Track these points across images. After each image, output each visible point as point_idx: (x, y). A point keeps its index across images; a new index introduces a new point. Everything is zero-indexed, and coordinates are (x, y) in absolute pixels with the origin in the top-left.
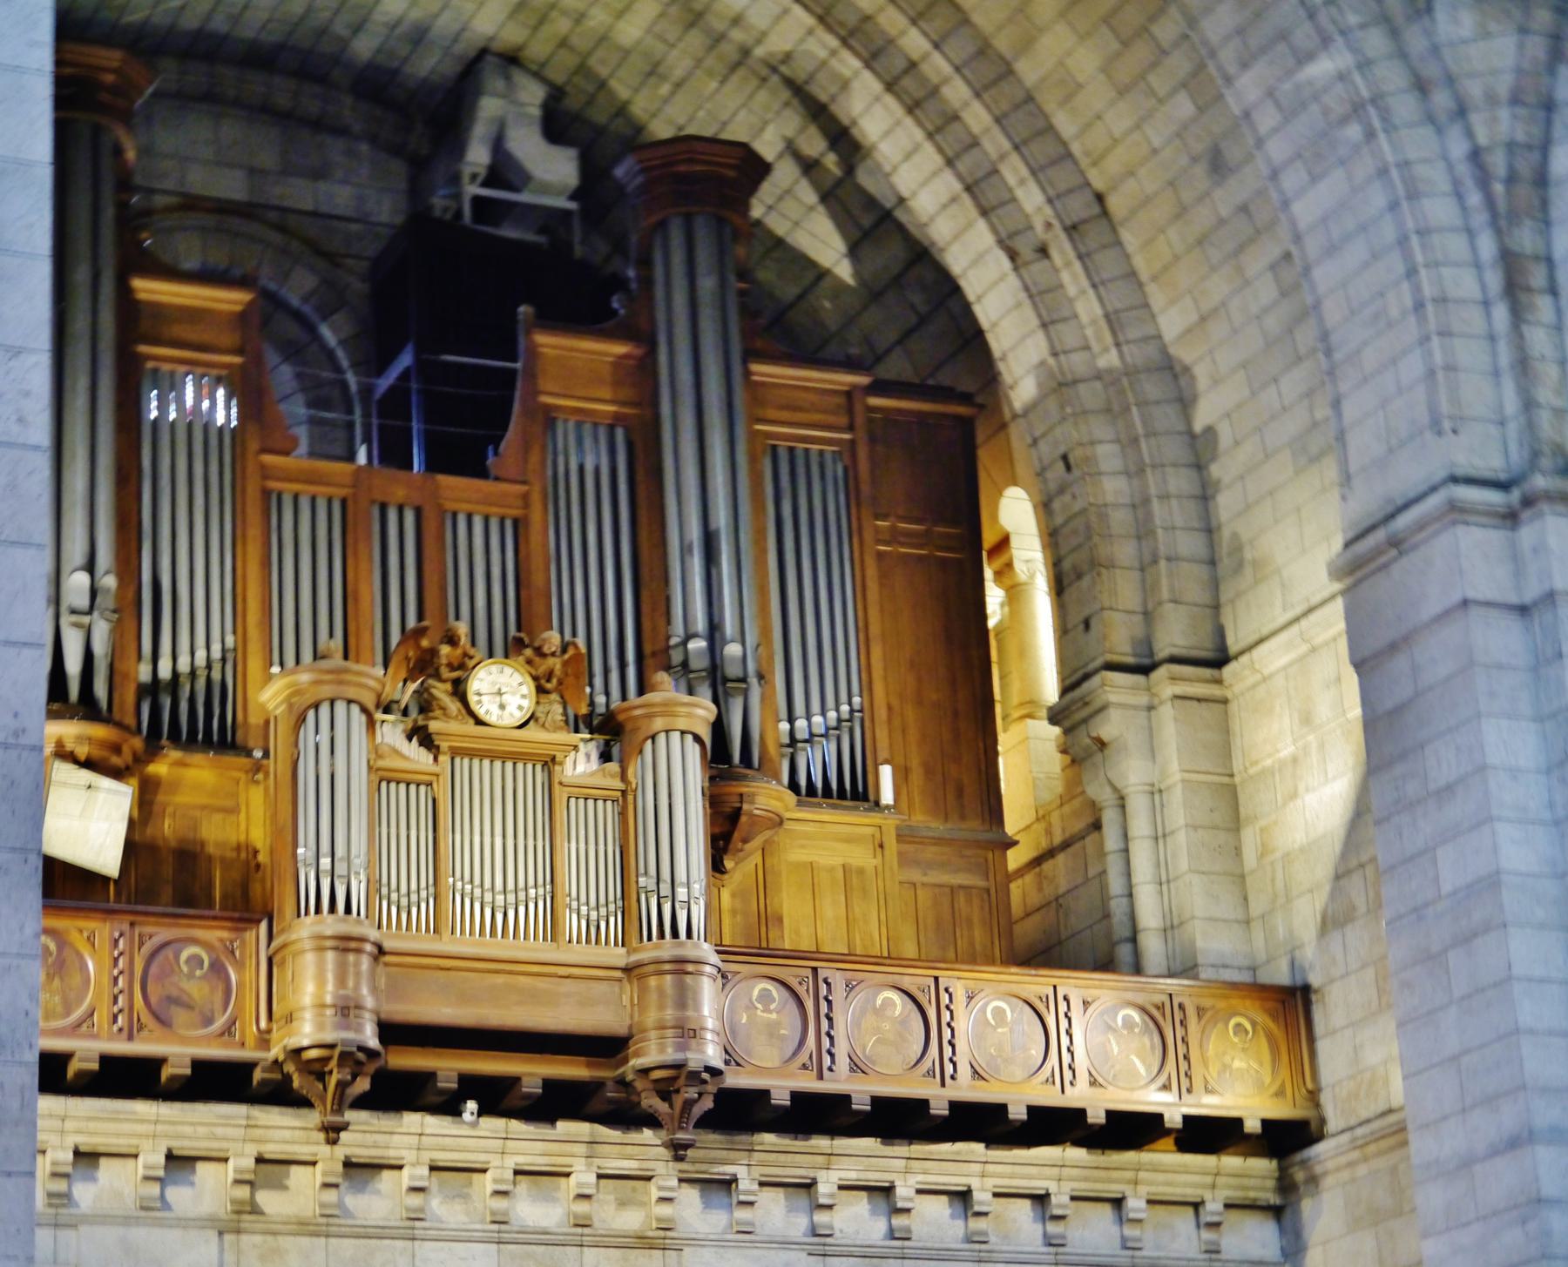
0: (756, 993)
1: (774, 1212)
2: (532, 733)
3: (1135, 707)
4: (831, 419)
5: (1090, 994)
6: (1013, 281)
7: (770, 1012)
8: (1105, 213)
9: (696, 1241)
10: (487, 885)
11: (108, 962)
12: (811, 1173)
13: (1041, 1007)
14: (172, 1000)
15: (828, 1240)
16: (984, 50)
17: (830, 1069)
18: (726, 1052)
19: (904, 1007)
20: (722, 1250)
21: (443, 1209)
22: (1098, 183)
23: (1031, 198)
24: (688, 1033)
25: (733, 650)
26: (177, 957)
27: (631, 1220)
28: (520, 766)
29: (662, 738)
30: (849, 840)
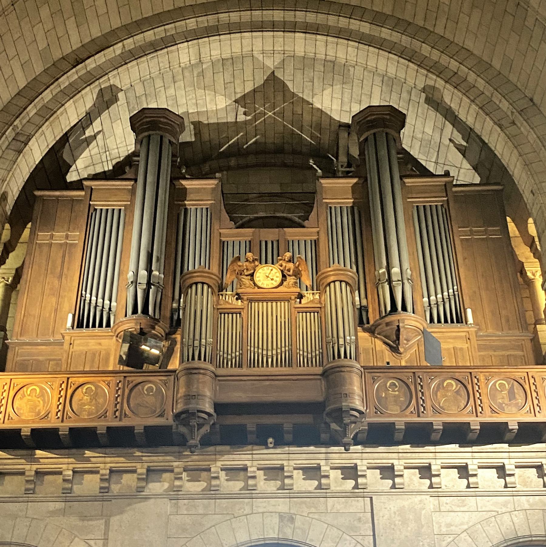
0: (388, 384)
2: (281, 289)
6: (502, 134)
7: (395, 391)
8: (534, 104)
10: (265, 347)
11: (114, 392)
13: (522, 382)
15: (439, 490)
16: (480, 60)
17: (423, 412)
18: (376, 409)
19: (457, 386)
20: (390, 497)
22: (529, 95)
23: (505, 105)
25: (395, 270)
26: (143, 389)
28: (279, 303)
29: (332, 285)
30: (455, 338)
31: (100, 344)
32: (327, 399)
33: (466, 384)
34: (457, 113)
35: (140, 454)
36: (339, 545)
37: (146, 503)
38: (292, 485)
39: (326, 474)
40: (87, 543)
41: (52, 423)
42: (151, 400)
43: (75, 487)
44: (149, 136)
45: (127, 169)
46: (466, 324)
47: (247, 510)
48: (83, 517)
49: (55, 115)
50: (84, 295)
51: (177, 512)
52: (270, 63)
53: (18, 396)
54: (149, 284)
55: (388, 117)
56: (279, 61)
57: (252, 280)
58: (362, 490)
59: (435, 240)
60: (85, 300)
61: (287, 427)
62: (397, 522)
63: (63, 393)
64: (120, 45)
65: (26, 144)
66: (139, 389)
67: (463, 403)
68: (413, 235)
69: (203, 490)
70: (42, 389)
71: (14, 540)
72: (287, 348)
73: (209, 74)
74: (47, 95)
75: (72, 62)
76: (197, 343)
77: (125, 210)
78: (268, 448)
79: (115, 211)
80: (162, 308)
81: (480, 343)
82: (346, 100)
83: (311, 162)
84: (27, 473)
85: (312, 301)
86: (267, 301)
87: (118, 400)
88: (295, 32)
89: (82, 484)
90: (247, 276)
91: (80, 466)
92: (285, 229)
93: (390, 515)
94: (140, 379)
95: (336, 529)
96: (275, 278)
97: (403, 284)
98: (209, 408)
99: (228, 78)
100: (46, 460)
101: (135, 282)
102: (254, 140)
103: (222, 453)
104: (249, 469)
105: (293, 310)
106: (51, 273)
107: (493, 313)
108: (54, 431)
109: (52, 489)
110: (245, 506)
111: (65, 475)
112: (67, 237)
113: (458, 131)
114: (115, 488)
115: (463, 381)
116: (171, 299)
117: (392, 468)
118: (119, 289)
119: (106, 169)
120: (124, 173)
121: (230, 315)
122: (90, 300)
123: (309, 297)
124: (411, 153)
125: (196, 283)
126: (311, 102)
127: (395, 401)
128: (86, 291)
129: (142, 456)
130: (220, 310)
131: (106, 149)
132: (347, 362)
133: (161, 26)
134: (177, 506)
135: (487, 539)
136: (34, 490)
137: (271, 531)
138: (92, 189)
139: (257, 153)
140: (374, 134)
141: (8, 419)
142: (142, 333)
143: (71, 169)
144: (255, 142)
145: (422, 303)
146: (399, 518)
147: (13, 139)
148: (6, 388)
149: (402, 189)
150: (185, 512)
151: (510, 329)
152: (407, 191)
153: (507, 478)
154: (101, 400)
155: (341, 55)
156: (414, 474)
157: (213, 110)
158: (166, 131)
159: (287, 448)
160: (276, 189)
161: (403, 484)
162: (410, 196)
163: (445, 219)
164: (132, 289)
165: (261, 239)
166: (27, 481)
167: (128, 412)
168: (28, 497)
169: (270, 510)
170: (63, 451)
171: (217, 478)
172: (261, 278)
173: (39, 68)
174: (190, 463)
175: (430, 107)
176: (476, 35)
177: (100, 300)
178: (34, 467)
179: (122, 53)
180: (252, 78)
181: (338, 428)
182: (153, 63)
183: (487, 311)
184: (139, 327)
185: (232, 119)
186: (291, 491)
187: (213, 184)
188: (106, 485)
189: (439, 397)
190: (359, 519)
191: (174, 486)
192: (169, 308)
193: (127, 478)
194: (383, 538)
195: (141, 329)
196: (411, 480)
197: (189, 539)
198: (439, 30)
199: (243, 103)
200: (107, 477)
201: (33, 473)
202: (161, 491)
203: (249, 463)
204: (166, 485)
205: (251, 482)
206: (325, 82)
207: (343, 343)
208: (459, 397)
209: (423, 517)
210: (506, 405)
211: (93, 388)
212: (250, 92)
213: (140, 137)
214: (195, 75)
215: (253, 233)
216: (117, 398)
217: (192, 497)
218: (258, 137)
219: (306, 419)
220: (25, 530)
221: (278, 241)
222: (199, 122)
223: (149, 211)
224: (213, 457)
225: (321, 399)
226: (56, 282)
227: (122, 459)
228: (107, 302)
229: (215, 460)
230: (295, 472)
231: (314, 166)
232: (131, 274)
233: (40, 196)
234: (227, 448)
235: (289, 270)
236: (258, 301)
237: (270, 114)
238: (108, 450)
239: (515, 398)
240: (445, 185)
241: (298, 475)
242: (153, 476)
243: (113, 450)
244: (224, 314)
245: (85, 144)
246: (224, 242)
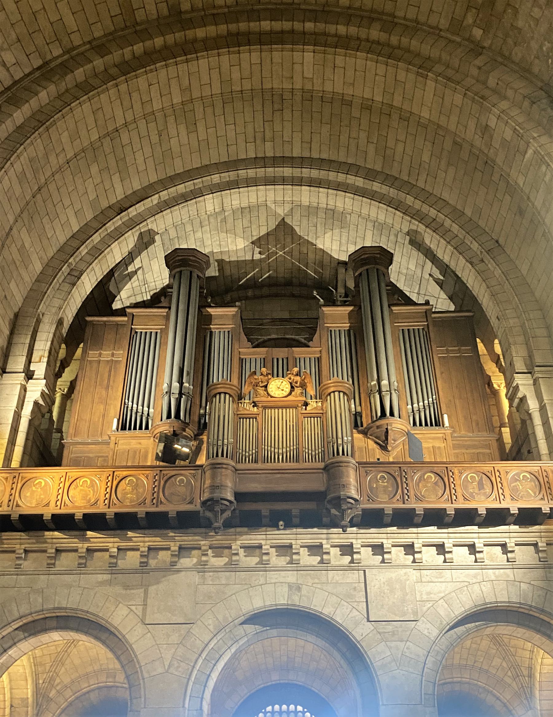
0: (379, 477)
3: (528, 385)
4: (421, 320)
5: (508, 469)
6: (473, 270)
7: (385, 483)
8: (499, 245)
10: (277, 446)
11: (152, 483)
13: (489, 475)
15: (421, 564)
16: (455, 209)
17: (407, 500)
19: (435, 478)
20: (380, 570)
22: (495, 238)
23: (475, 246)
25: (385, 382)
26: (176, 481)
29: (332, 394)
30: (434, 438)
31: (140, 443)
32: (328, 489)
33: (443, 476)
34: (435, 253)
35: (173, 534)
36: (338, 610)
37: (178, 575)
38: (299, 560)
39: (327, 551)
40: (129, 608)
41: (101, 509)
42: (182, 490)
43: (119, 562)
44: (181, 272)
45: (163, 299)
46: (443, 427)
47: (262, 581)
48: (126, 587)
49: (103, 255)
50: (126, 403)
51: (204, 582)
52: (280, 211)
53: (73, 486)
54: (181, 394)
55: (378, 256)
56: (288, 209)
57: (266, 390)
58: (357, 565)
59: (417, 357)
60: (128, 407)
61: (295, 512)
62: (386, 591)
63: (109, 484)
64: (157, 196)
65: (79, 278)
66: (172, 481)
67: (440, 493)
68: (399, 353)
69: (225, 565)
70: (92, 481)
72: (295, 447)
73: (230, 220)
74: (96, 238)
75: (117, 210)
76: (220, 443)
77: (161, 332)
78: (279, 529)
79: (153, 334)
80: (192, 414)
81: (454, 442)
82: (343, 241)
83: (315, 293)
84: (80, 551)
85: (315, 408)
86: (278, 408)
87: (155, 490)
88: (301, 185)
89: (125, 559)
90: (261, 387)
91: (123, 544)
92: (293, 349)
93: (380, 585)
94: (173, 473)
95: (335, 597)
96: (285, 389)
97: (391, 394)
98: (230, 496)
99: (246, 224)
100: (95, 540)
101: (169, 393)
102: (267, 275)
103: (241, 534)
104: (263, 547)
105: (300, 415)
106: (100, 385)
107: (465, 418)
108: (102, 516)
109: (101, 564)
110: (260, 577)
111: (111, 552)
112: (113, 355)
113: (436, 267)
114: (153, 563)
115: (441, 474)
116: (199, 406)
117: (382, 546)
118: (156, 398)
119: (145, 299)
120: (160, 302)
121: (248, 420)
122: (132, 407)
123: (313, 405)
124: (398, 285)
125: (220, 393)
126: (315, 243)
127: (385, 491)
128: (128, 400)
129: (175, 536)
130: (239, 416)
131: (145, 283)
132: (344, 459)
133: (191, 180)
134: (204, 578)
135: (460, 605)
136: (85, 564)
137: (281, 598)
138: (133, 315)
139: (270, 286)
140: (367, 270)
141: (64, 506)
142: (175, 434)
143: (116, 299)
144: (269, 277)
145: (407, 409)
146: (387, 588)
147: (68, 274)
148: (62, 479)
149: (390, 315)
150: (211, 583)
151: (479, 431)
152: (394, 317)
153: (477, 554)
155: (340, 205)
156: (400, 551)
157: (233, 250)
158: (195, 267)
159: (295, 530)
160: (286, 315)
161: (390, 559)
162: (396, 321)
163: (426, 340)
164: (166, 398)
165: (274, 357)
166: (80, 557)
167: (163, 499)
169: (281, 581)
170: (109, 532)
171: (237, 554)
172: (274, 389)
173: (89, 216)
174: (214, 542)
175: (413, 248)
176: (451, 188)
177: (140, 407)
178: (86, 545)
179: (158, 203)
180: (266, 224)
181: (337, 513)
182: (184, 211)
183: (460, 416)
184: (172, 430)
185: (248, 257)
186: (298, 565)
187: (233, 311)
188: (145, 560)
189: (420, 487)
190: (355, 589)
191: (201, 561)
192: (197, 414)
193: (162, 554)
194: (374, 604)
195: (174, 431)
196: (397, 555)
197: (212, 605)
198: (421, 184)
199: (258, 245)
200: (146, 553)
201: (85, 550)
202: (190, 565)
203: (263, 542)
204: (195, 560)
205: (265, 558)
206: (327, 227)
207: (341, 443)
208: (437, 487)
209: (407, 587)
210: (476, 494)
211: (135, 480)
212: (264, 235)
213: (173, 272)
214: (219, 221)
215: (267, 351)
216: (154, 488)
217: (216, 570)
218: (271, 272)
219: (311, 506)
220: (78, 597)
221: (287, 358)
222: (222, 260)
223: (181, 333)
224: (234, 537)
225: (323, 489)
226: (104, 392)
227: (158, 539)
228: (146, 409)
229: (236, 540)
230: (302, 549)
231: (318, 296)
232: (165, 385)
233: (91, 321)
234: (246, 529)
235: (296, 383)
236: (271, 408)
237: (281, 253)
238: (146, 531)
239: (483, 488)
240: (426, 312)
241: (304, 552)
242: (183, 553)
243: (151, 531)
245: (128, 278)
246: (242, 359)
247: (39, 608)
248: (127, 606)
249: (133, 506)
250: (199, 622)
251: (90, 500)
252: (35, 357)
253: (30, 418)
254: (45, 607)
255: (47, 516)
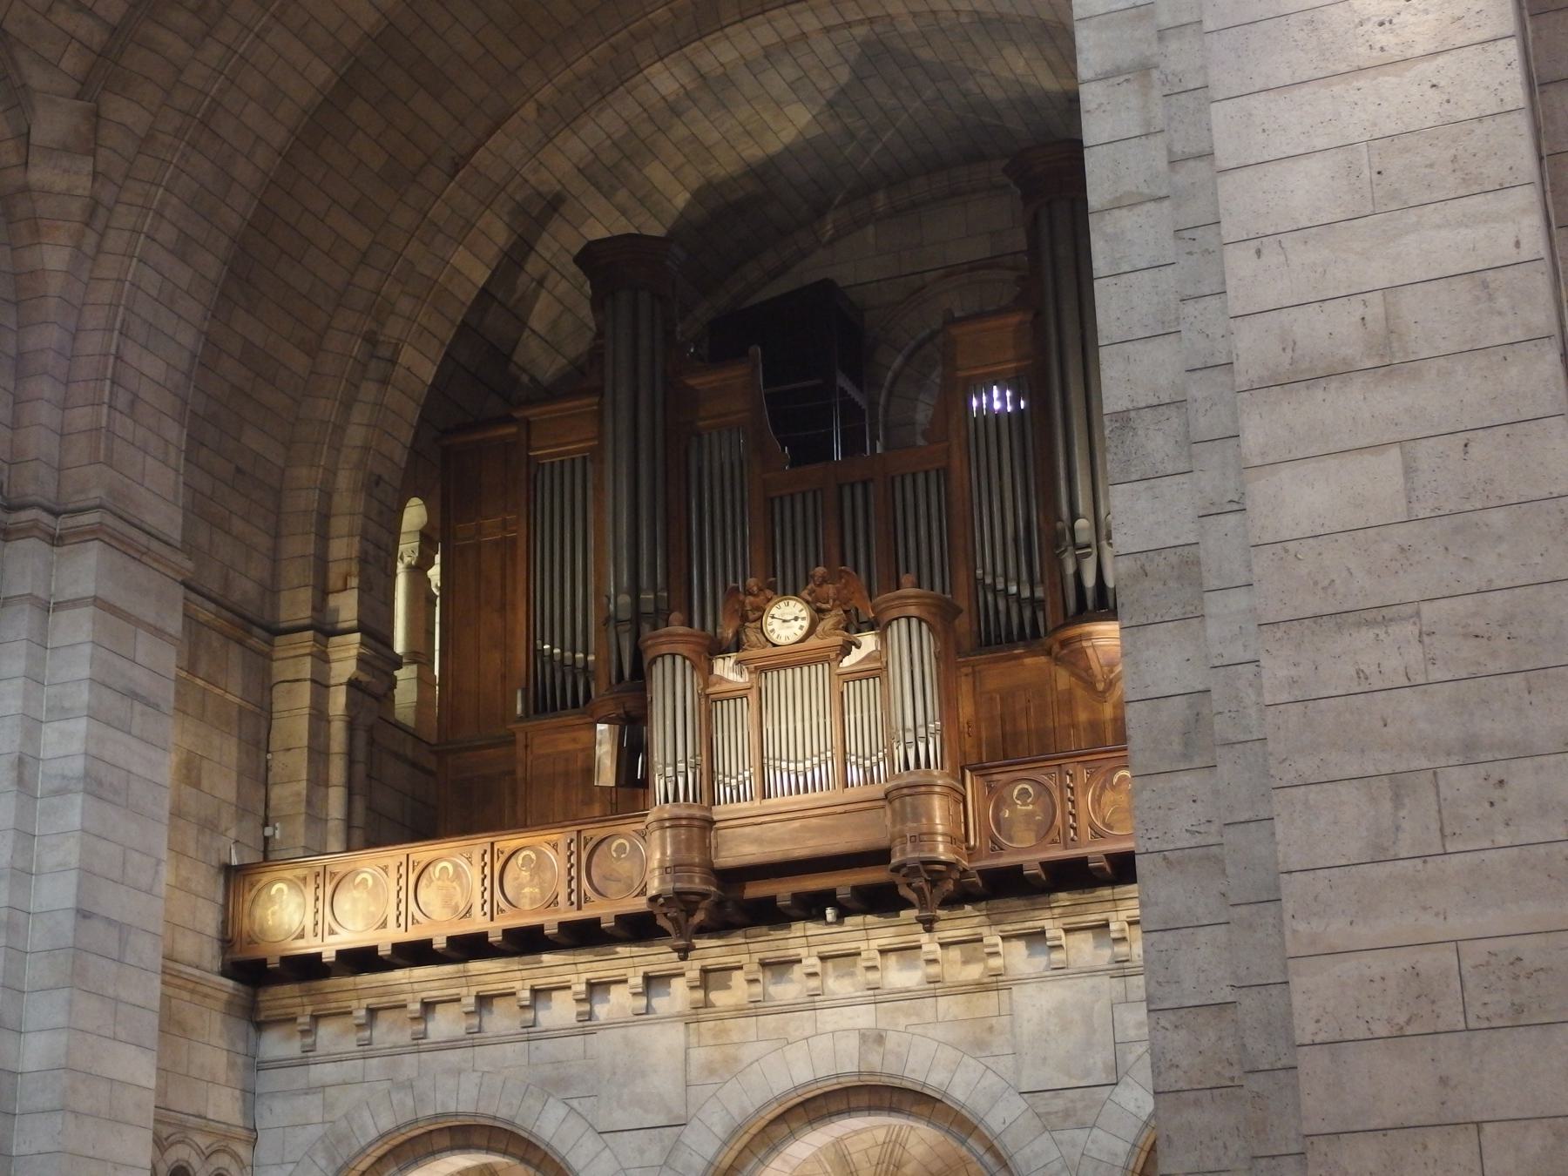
0: (1016, 792)
1: (1083, 949)
2: (813, 642)
9: (1021, 981)
12: (1104, 916)
14: (606, 878)
15: (1126, 964)
20: (1041, 984)
21: (838, 986)
24: (924, 837)
27: (974, 972)
31: (574, 740)
36: (957, 1075)
41: (478, 923)
47: (809, 1031)
51: (699, 1042)
70: (456, 866)
71: (461, 1109)
78: (828, 924)
79: (577, 461)
91: (541, 983)
111: (519, 1000)
114: (602, 1011)
121: (732, 702)
125: (663, 656)
130: (712, 696)
138: (528, 423)
150: (712, 1043)
154: (548, 875)
168: (473, 1039)
178: (474, 990)
184: (622, 711)
190: (991, 1029)
193: (619, 995)
197: (718, 1086)
207: (913, 740)
211: (533, 856)
244: (722, 701)
247: (409, 1117)
248: (565, 1101)
249: (535, 912)
250: (695, 1122)
251: (456, 908)
252: (334, 580)
253: (348, 719)
254: (420, 1115)
255: (385, 950)
